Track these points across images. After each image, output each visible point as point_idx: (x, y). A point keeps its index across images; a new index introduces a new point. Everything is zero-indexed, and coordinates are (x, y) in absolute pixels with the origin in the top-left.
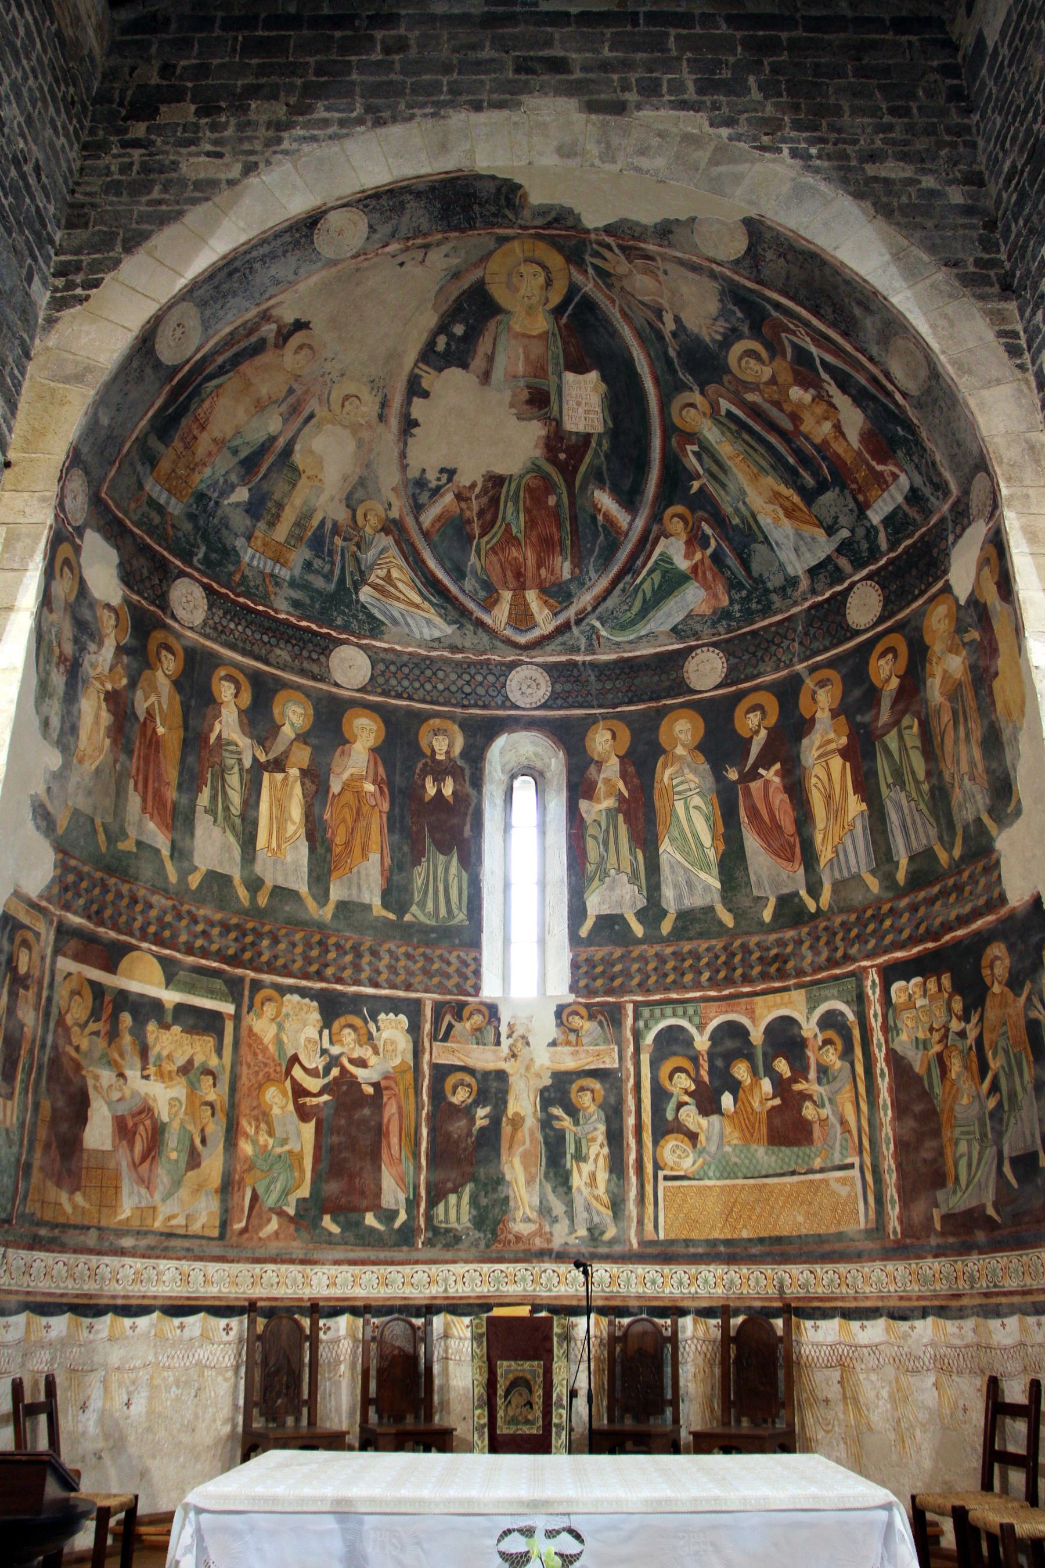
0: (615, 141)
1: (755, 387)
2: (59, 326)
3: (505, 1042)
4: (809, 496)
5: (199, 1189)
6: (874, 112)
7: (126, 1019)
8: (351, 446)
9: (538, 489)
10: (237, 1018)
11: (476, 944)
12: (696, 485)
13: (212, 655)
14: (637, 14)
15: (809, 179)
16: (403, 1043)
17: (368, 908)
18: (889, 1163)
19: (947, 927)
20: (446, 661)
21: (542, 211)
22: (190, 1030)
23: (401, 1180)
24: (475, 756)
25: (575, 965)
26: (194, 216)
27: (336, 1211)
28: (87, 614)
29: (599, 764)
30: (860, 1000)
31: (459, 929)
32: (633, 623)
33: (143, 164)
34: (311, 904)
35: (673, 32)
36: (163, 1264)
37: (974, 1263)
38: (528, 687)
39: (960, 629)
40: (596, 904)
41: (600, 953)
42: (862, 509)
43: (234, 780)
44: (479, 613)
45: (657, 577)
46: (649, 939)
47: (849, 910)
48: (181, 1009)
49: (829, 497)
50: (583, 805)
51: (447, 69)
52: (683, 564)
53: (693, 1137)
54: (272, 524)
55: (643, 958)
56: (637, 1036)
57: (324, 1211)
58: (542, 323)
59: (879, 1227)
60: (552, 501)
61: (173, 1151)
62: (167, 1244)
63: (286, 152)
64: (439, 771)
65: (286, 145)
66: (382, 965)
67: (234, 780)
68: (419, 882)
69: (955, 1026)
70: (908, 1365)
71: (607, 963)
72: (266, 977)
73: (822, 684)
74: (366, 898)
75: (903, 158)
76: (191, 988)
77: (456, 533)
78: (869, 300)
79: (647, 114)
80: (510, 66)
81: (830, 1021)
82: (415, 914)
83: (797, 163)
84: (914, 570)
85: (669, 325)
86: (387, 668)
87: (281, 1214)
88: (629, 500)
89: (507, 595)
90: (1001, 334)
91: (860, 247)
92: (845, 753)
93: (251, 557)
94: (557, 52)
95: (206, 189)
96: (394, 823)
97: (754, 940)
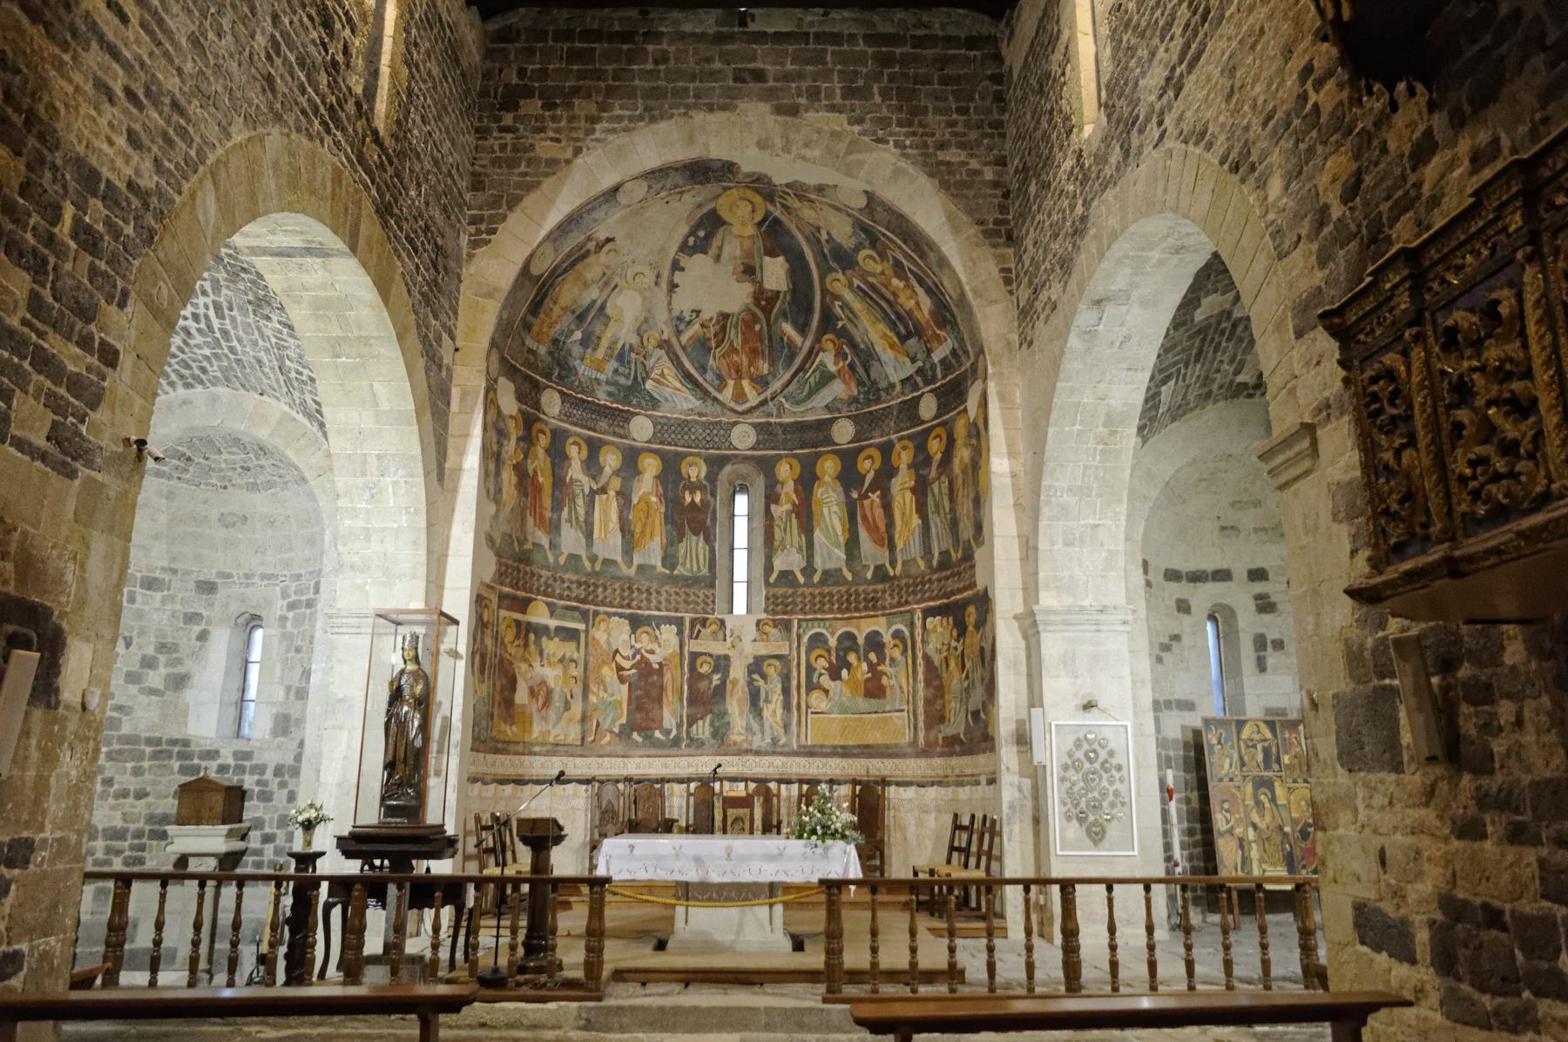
0: (792, 136)
1: (873, 275)
2: (475, 260)
3: (729, 640)
4: (903, 339)
5: (570, 721)
6: (947, 112)
7: (532, 637)
8: (639, 300)
9: (749, 322)
10: (587, 631)
11: (713, 586)
12: (840, 324)
13: (566, 431)
14: (808, 34)
15: (903, 164)
16: (675, 641)
17: (654, 567)
18: (921, 710)
19: (953, 593)
20: (696, 422)
21: (748, 175)
22: (564, 640)
23: (673, 713)
24: (712, 477)
25: (767, 598)
26: (547, 184)
27: (640, 730)
28: (501, 425)
29: (783, 484)
30: (912, 625)
31: (704, 578)
32: (803, 401)
33: (513, 145)
34: (624, 567)
35: (830, 49)
36: (555, 759)
37: (955, 761)
38: (743, 437)
39: (969, 436)
40: (779, 564)
41: (780, 591)
42: (929, 352)
43: (580, 501)
44: (715, 393)
45: (818, 374)
46: (808, 584)
47: (908, 576)
48: (558, 629)
49: (912, 342)
50: (773, 507)
51: (693, 78)
52: (833, 368)
53: (827, 692)
54: (595, 349)
55: (803, 595)
56: (799, 637)
57: (633, 730)
58: (751, 230)
59: (914, 742)
60: (757, 328)
61: (557, 702)
62: (556, 749)
63: (597, 140)
64: (692, 488)
65: (597, 135)
66: (662, 599)
67: (580, 501)
68: (682, 552)
69: (954, 644)
70: (924, 810)
72: (601, 609)
73: (904, 448)
74: (653, 562)
75: (961, 146)
76: (563, 618)
77: (702, 346)
78: (932, 246)
79: (811, 115)
80: (731, 75)
81: (897, 635)
82: (680, 570)
83: (897, 151)
84: (952, 395)
85: (824, 237)
86: (662, 427)
87: (612, 732)
88: (802, 329)
89: (731, 383)
90: (1003, 270)
91: (928, 209)
92: (913, 490)
93: (584, 370)
94: (758, 65)
95: (553, 163)
96: (668, 519)
97: (861, 588)
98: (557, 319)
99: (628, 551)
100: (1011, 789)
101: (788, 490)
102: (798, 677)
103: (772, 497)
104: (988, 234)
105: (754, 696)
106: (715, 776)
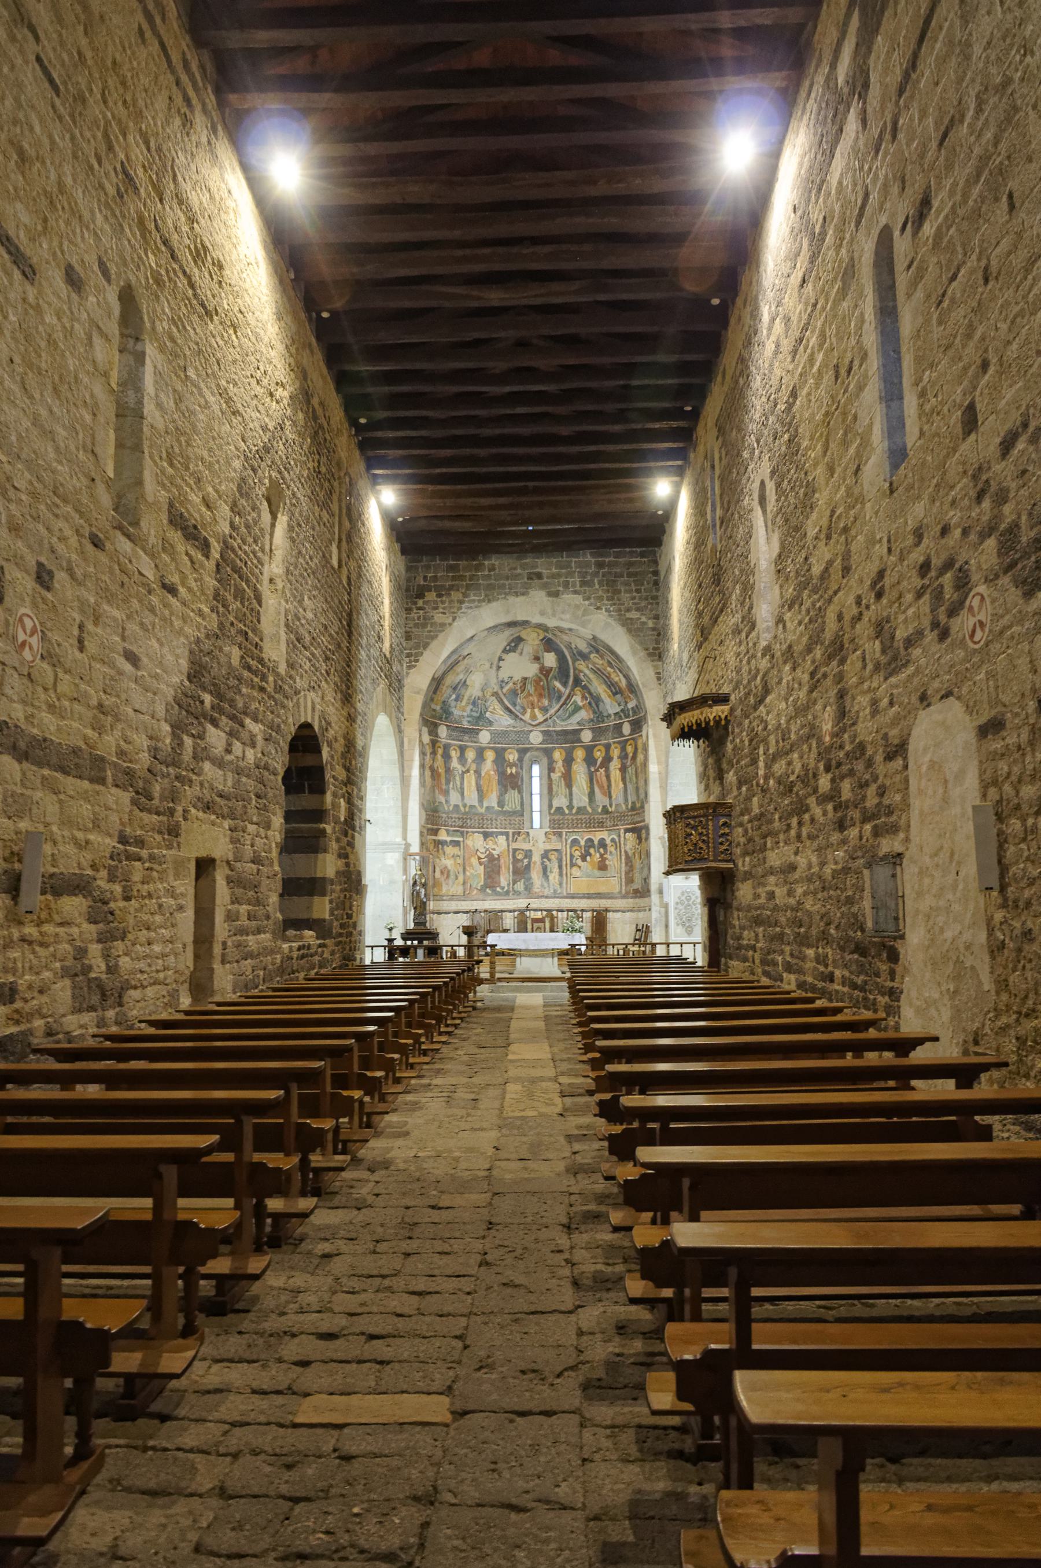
6: (630, 591)
9: (537, 681)
16: (505, 843)
26: (441, 636)
38: (536, 738)
40: (556, 804)
46: (570, 814)
51: (507, 578)
52: (581, 704)
58: (537, 642)
61: (452, 876)
62: (453, 898)
64: (511, 765)
71: (558, 821)
75: (637, 609)
77: (514, 693)
81: (613, 840)
82: (506, 808)
84: (637, 725)
86: (496, 736)
88: (565, 684)
91: (622, 643)
93: (456, 712)
96: (500, 782)
98: (445, 691)
99: (481, 800)
100: (655, 914)
101: (559, 766)
102: (566, 860)
103: (551, 769)
104: (650, 655)
105: (545, 870)
106: (527, 909)
